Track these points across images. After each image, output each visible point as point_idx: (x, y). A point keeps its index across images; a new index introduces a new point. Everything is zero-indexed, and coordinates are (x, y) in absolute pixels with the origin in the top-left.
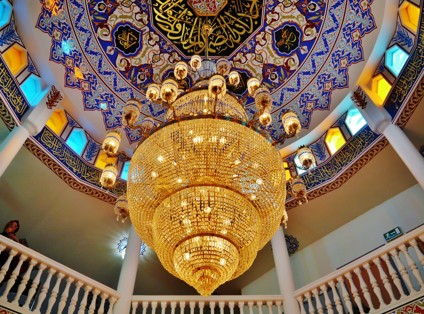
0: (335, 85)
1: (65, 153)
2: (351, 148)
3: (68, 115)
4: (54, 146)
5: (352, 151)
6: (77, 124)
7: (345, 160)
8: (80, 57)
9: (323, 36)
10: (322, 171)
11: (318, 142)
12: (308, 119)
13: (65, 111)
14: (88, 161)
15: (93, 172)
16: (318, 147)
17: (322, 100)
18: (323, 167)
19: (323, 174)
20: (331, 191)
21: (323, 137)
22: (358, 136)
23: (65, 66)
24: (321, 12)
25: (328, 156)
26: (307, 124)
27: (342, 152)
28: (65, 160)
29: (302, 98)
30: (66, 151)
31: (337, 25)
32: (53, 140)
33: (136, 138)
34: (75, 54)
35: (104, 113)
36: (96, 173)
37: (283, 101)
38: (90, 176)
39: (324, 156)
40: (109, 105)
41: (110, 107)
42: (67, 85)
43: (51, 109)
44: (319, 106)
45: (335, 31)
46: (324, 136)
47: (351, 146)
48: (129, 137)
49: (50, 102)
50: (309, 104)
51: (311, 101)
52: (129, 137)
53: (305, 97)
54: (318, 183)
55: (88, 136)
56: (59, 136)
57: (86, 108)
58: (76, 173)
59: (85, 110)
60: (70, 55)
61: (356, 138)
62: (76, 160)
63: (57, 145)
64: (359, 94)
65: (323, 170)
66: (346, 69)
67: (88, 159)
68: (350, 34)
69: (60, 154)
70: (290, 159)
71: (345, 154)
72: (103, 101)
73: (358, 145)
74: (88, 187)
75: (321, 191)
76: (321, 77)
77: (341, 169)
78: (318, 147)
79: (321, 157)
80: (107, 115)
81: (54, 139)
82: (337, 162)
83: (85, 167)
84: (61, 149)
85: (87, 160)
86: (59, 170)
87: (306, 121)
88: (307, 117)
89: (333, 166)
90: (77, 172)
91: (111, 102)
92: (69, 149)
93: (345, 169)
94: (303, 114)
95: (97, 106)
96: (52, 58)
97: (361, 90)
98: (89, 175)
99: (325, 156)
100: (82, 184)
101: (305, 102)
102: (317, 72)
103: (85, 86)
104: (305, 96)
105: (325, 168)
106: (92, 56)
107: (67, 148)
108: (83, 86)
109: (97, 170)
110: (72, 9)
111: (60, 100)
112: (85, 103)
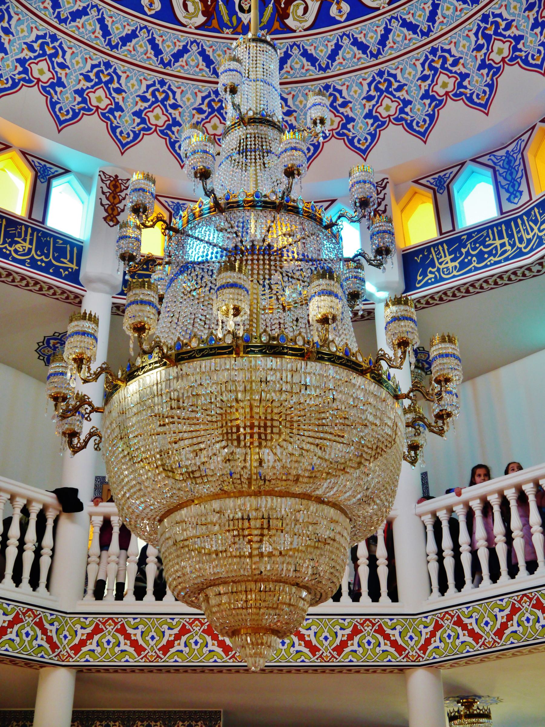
11: (510, 148)
16: (509, 162)
21: (523, 138)
39: (518, 191)
75: (498, 280)
78: (509, 162)
79: (512, 193)
99: (521, 193)
103: (41, 72)
108: (36, 74)
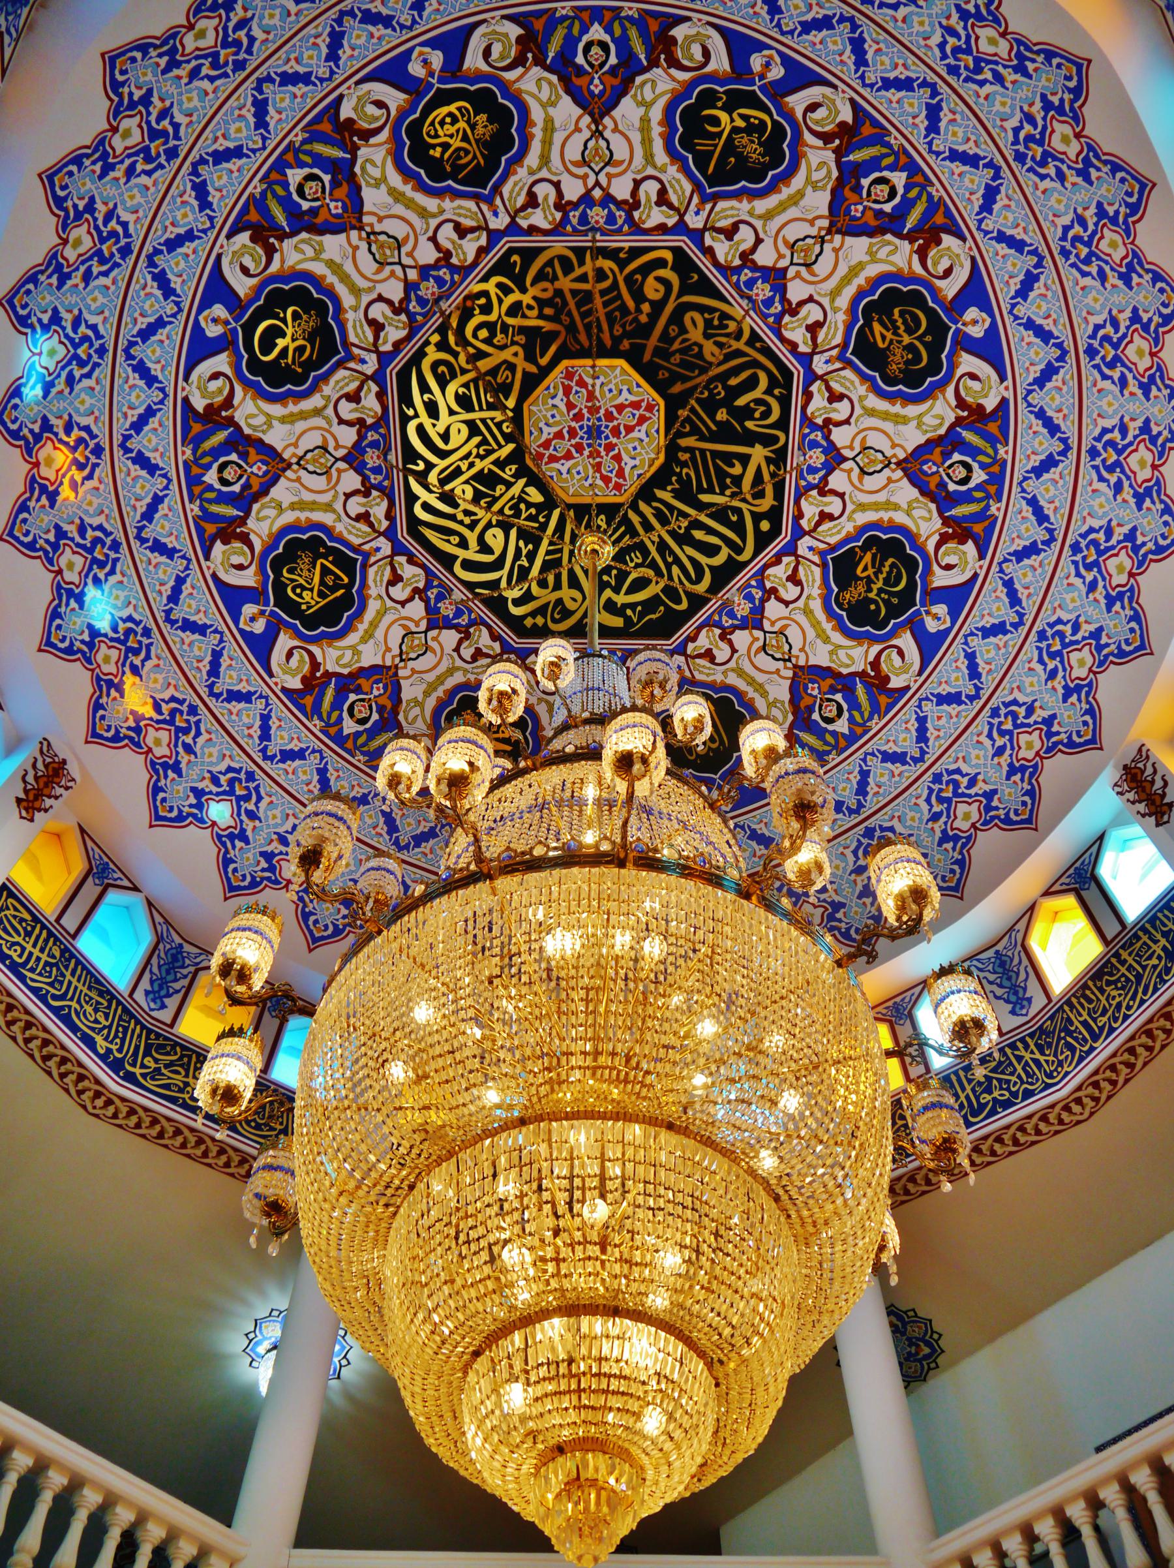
0: (1054, 739)
1: (70, 983)
2: (1123, 970)
3: (90, 844)
4: (31, 954)
5: (1128, 980)
6: (118, 875)
7: (1103, 1014)
8: (145, 641)
9: (1001, 571)
10: (1019, 1059)
11: (1000, 947)
12: (961, 863)
13: (82, 831)
14: (153, 1014)
15: (168, 1054)
16: (1002, 964)
17: (1010, 794)
18: (1022, 1040)
19: (1024, 1069)
20: (1057, 1132)
22: (1148, 926)
23: (93, 670)
24: (992, 489)
25: (1039, 1001)
26: (959, 880)
27: (1090, 983)
28: (70, 1007)
29: (936, 787)
30: (73, 974)
31: (1050, 531)
32: (28, 934)
33: (331, 928)
34: (128, 632)
35: (219, 837)
36: (180, 1059)
37: (868, 798)
38: (158, 1070)
39: (1023, 999)
40: (239, 807)
41: (244, 817)
42: (94, 736)
43: (32, 820)
44: (998, 817)
45: (1043, 554)
46: (1021, 926)
47: (1123, 962)
48: (307, 926)
49: (31, 797)
50: (962, 809)
51: (970, 796)
52: (307, 926)
53: (948, 783)
54: (1007, 1104)
55: (158, 919)
56: (52, 919)
57: (159, 818)
58: (103, 1058)
59: (151, 826)
60: (111, 634)
61: (1140, 933)
62: (109, 1007)
63: (42, 950)
64: (1143, 772)
65: (1022, 1053)
66: (1090, 685)
67: (152, 1005)
68: (1095, 563)
69: (51, 984)
70: (897, 1010)
71: (1102, 991)
72: (218, 794)
73: (1150, 958)
74: (146, 1109)
75: (1019, 1135)
76: (1003, 711)
77: (1092, 1049)
78: (1002, 964)
79: (1015, 1004)
80: (229, 845)
81: (34, 928)
82: (1076, 1023)
83: (140, 1036)
84: (56, 965)
85: (146, 1008)
86: (46, 1043)
87: (953, 871)
88: (957, 856)
89: (1059, 1039)
90: (109, 1051)
91: (247, 798)
92: (84, 968)
93: (1105, 1050)
94: (940, 845)
95: (195, 811)
96: (47, 645)
97: (1148, 757)
98: (153, 1065)
99: (1029, 1000)
100: (123, 1099)
101: (948, 801)
102: (985, 694)
103: (158, 742)
104: (945, 778)
105: (1032, 1047)
106: (188, 637)
107: (78, 962)
108: (150, 741)
109: (183, 1048)
110: (129, 479)
111: (67, 788)
112: (155, 800)
